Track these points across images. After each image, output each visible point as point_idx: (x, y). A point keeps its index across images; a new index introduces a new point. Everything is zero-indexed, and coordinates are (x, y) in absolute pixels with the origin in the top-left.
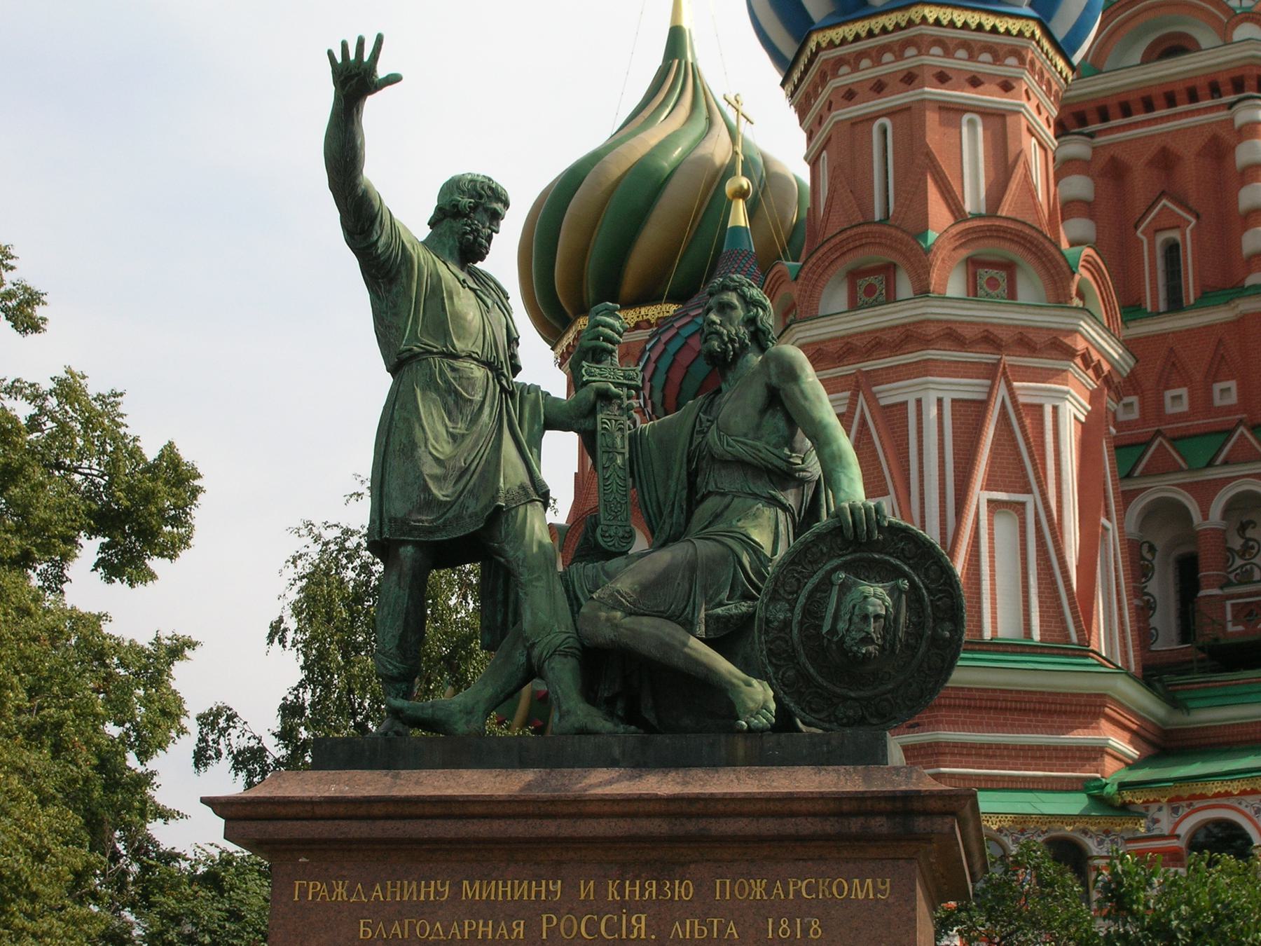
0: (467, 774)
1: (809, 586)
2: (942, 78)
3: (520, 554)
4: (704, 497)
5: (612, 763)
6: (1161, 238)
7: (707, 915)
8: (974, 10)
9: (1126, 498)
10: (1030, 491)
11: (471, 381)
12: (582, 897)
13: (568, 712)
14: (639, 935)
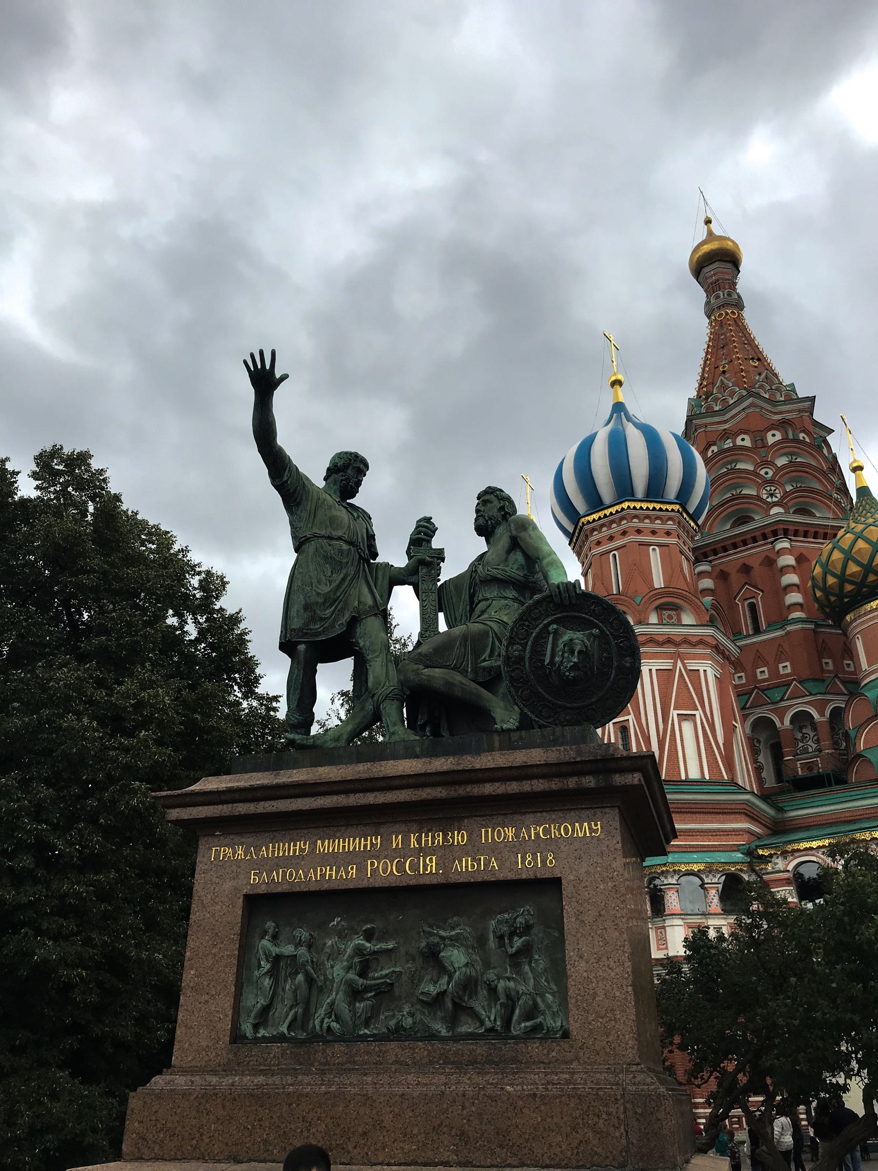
0: (321, 769)
1: (534, 635)
2: (639, 531)
3: (367, 644)
4: (477, 605)
5: (417, 757)
6: (747, 603)
7: (476, 854)
8: (651, 502)
9: (744, 718)
10: (697, 710)
11: (341, 551)
12: (394, 846)
13: (393, 733)
14: (431, 871)
